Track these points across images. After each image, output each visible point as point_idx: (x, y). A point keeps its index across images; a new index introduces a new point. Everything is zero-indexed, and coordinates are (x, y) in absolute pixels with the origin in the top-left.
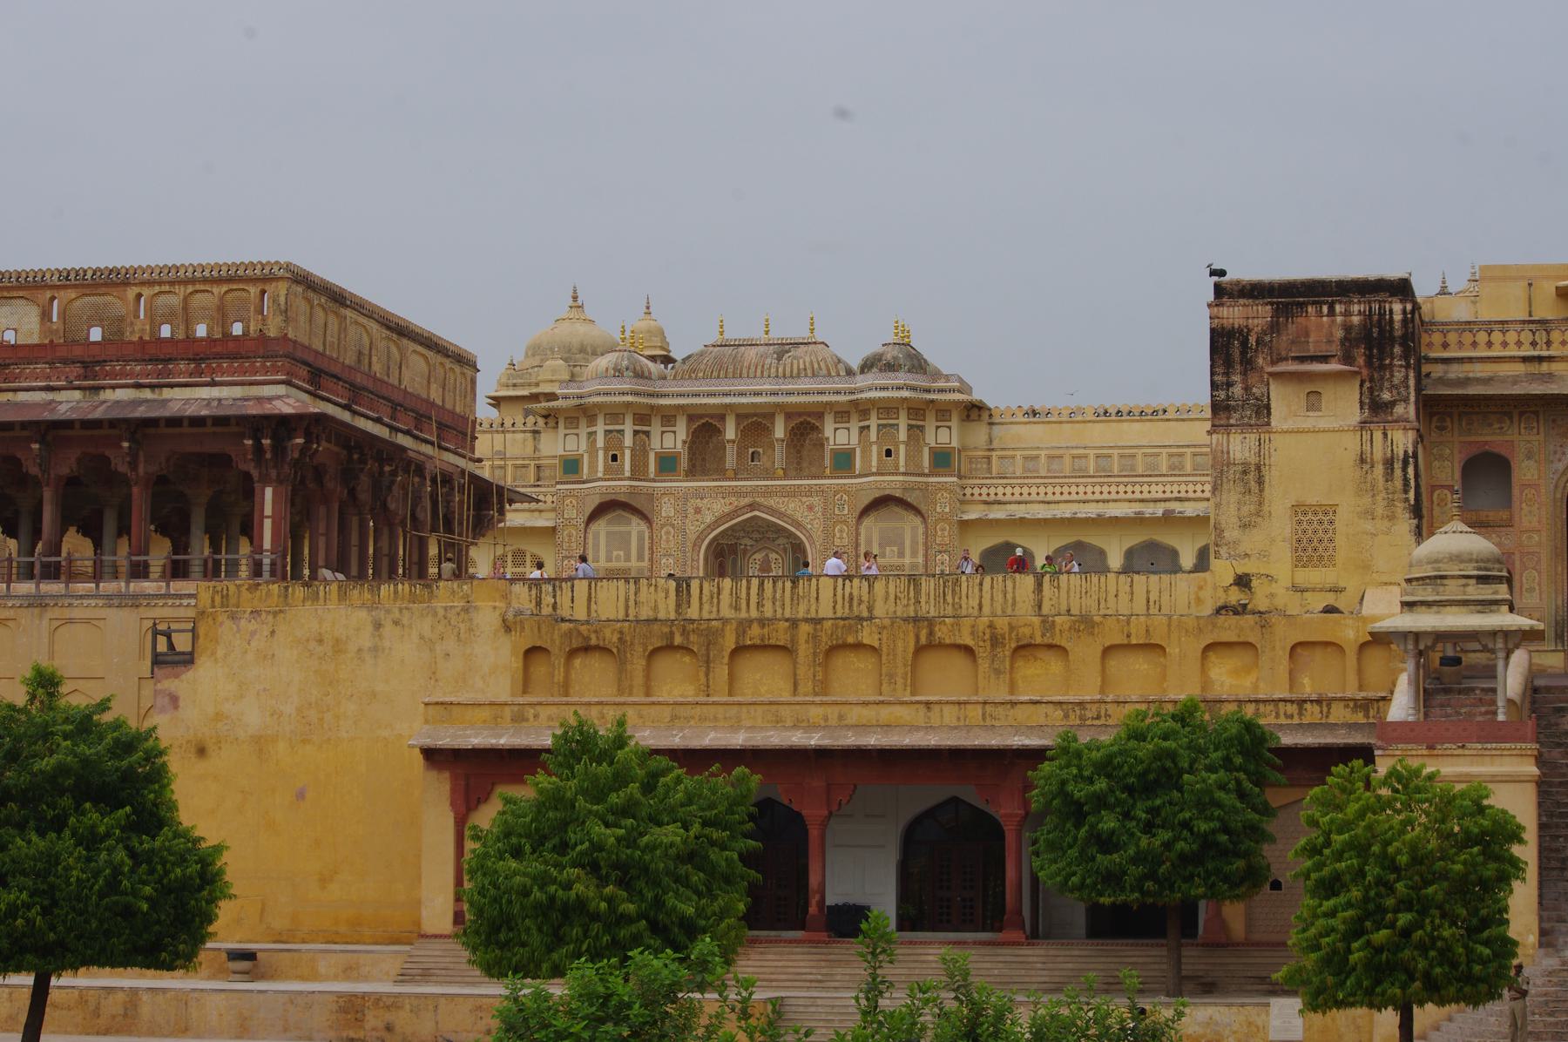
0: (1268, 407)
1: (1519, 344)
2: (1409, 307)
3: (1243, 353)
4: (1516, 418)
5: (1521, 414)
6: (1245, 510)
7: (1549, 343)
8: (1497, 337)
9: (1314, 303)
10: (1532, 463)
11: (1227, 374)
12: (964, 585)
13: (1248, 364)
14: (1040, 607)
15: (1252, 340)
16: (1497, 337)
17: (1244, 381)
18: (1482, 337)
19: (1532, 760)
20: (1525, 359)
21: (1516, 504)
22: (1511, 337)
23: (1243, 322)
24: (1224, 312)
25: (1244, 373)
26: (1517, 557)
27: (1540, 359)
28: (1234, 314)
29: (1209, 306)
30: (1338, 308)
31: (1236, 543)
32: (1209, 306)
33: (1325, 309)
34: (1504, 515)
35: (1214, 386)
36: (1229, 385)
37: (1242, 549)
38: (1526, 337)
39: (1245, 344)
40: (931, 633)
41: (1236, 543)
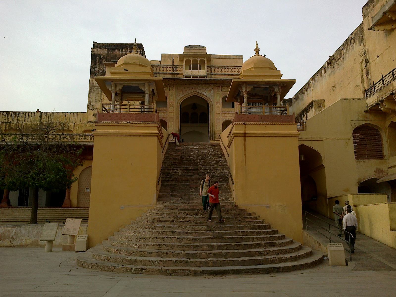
0: (105, 73)
1: (170, 70)
2: (142, 50)
3: (99, 60)
4: (169, 86)
5: (170, 86)
6: (97, 97)
7: (177, 71)
8: (165, 69)
9: (118, 49)
10: (172, 97)
11: (95, 65)
12: (21, 114)
13: (101, 63)
14: (41, 121)
15: (102, 57)
16: (165, 69)
17: (99, 67)
18: (161, 69)
19: (157, 128)
20: (171, 74)
21: (168, 106)
22: (168, 69)
23: (100, 53)
24: (95, 50)
25: (99, 65)
26: (168, 119)
27: (175, 74)
28: (98, 51)
29: (92, 48)
30: (124, 50)
31: (94, 106)
32: (92, 48)
33: (121, 50)
34: (165, 109)
35: (91, 67)
36: (95, 68)
37: (95, 107)
38: (171, 69)
39: (100, 58)
40: (9, 126)
41: (94, 106)
